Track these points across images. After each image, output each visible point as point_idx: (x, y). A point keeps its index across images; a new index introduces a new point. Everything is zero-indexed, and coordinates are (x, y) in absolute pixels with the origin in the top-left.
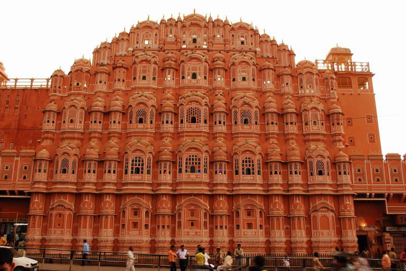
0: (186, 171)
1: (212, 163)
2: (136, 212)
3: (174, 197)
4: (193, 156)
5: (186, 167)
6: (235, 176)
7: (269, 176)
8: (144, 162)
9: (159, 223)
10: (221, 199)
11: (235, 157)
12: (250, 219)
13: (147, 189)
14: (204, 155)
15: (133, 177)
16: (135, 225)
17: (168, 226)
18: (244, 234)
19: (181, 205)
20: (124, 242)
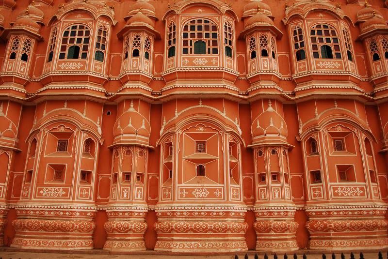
0: (185, 51)
1: (241, 39)
2: (63, 143)
3: (157, 108)
4: (200, 21)
5: (185, 43)
6: (296, 65)
7: (373, 64)
8: (91, 35)
9: (116, 168)
10: (270, 109)
11: (291, 26)
12: (345, 157)
13: (95, 90)
14: (225, 19)
15: (62, 66)
16: (59, 171)
17: (140, 177)
18: (336, 194)
19: (173, 125)
20: (26, 214)
